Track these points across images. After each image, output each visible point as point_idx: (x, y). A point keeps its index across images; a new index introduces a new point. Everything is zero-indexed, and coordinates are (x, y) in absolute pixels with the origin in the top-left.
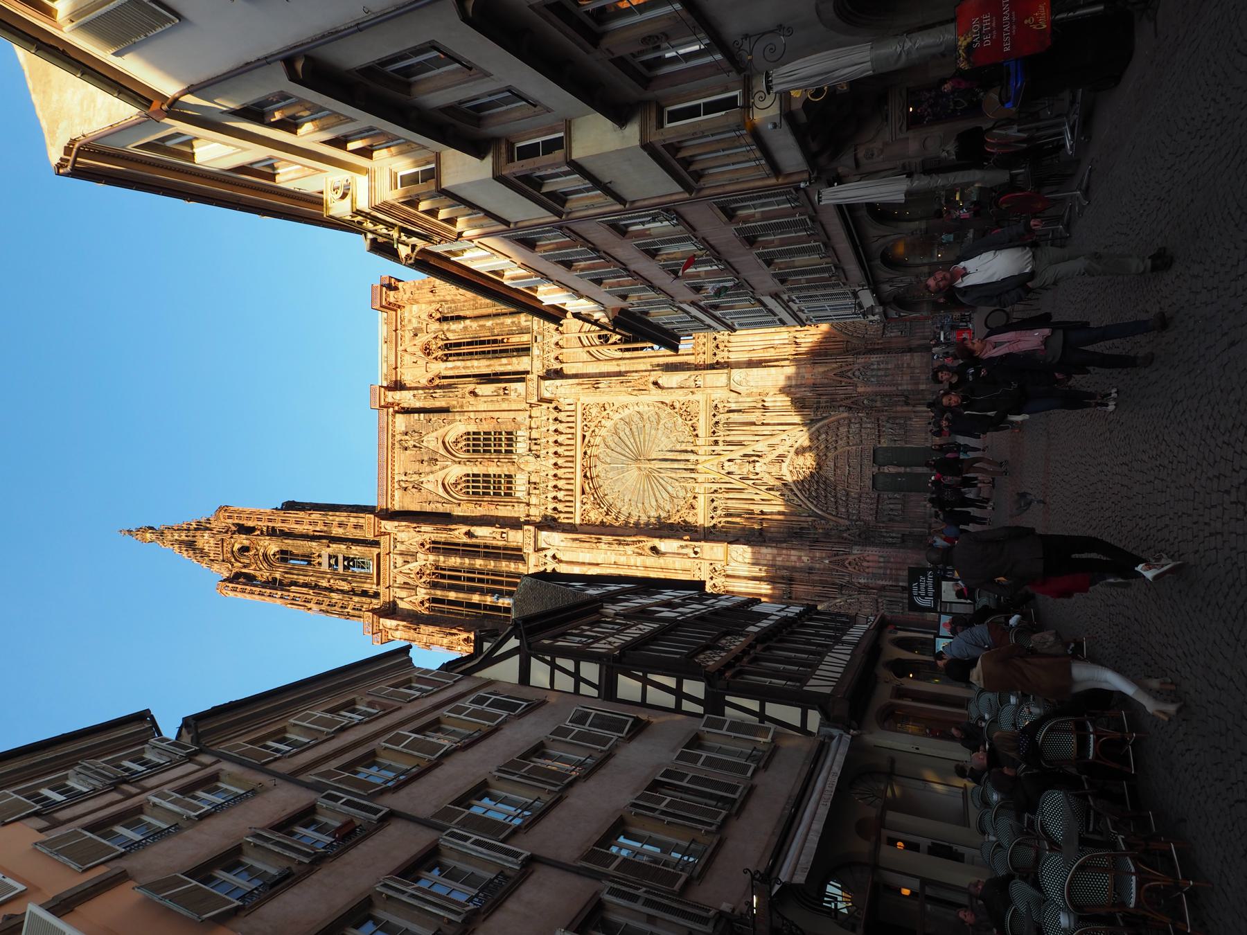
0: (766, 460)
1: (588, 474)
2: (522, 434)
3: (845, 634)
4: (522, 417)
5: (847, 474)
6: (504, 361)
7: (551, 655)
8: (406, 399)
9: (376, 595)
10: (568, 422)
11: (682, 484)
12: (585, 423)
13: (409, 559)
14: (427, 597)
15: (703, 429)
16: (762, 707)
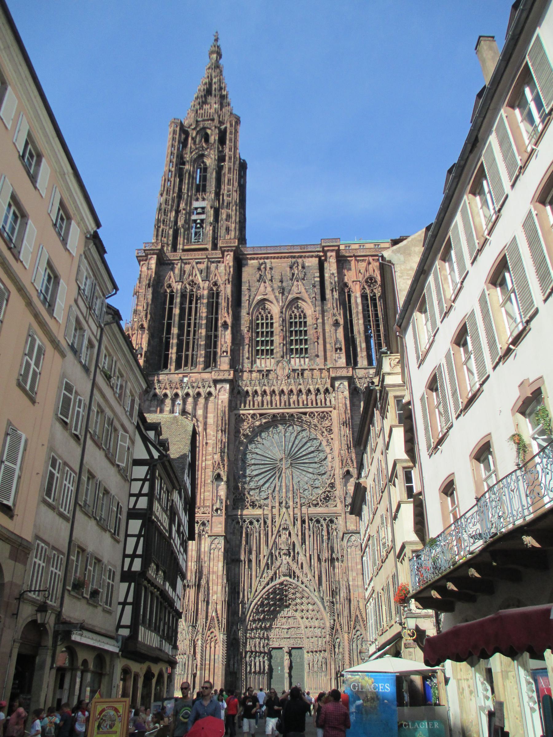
0: (291, 563)
1: (275, 419)
2: (306, 363)
3: (165, 641)
4: (320, 361)
5: (282, 627)
6: (364, 345)
7: (150, 479)
8: (331, 267)
9: (174, 249)
10: (316, 400)
11: (270, 496)
12: (316, 414)
13: (204, 274)
14: (175, 291)
15: (312, 510)
16: (129, 604)
